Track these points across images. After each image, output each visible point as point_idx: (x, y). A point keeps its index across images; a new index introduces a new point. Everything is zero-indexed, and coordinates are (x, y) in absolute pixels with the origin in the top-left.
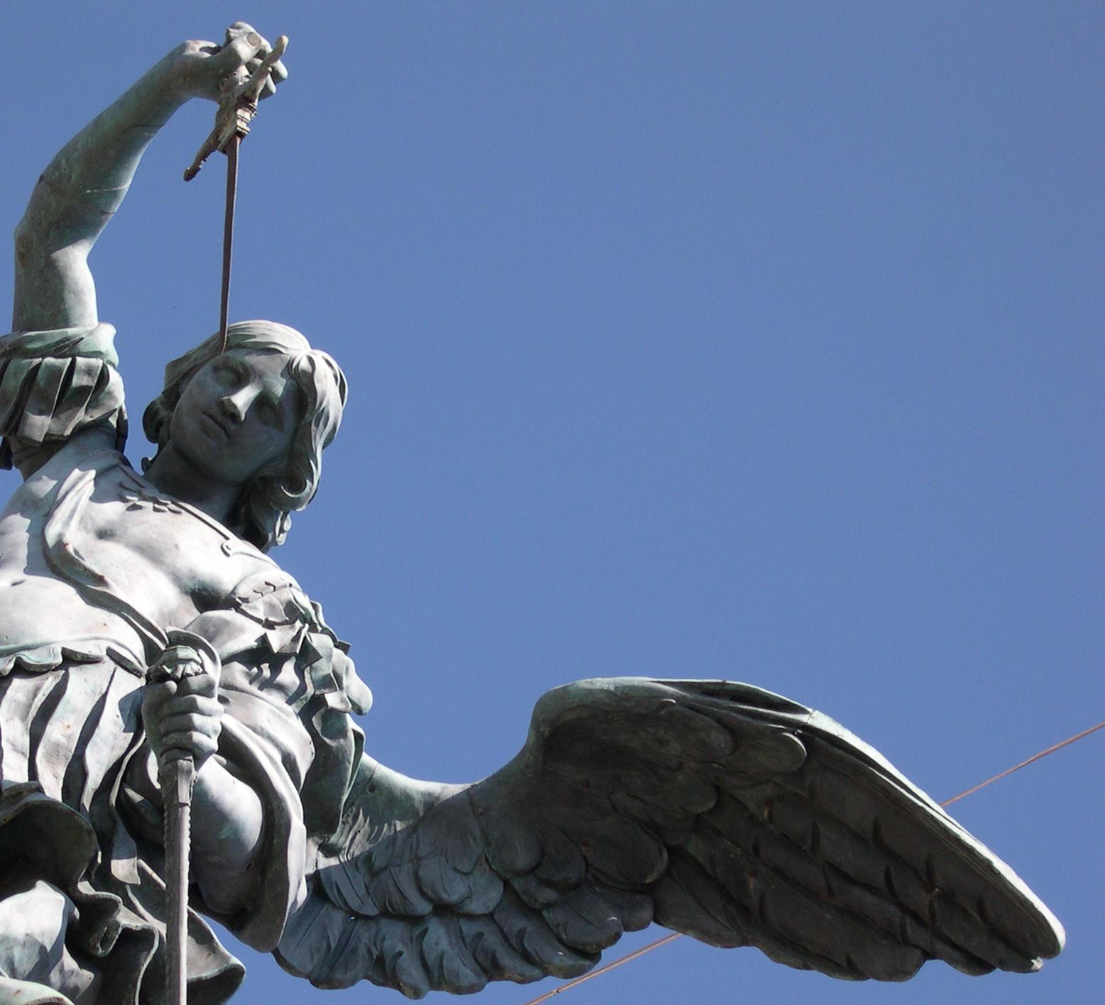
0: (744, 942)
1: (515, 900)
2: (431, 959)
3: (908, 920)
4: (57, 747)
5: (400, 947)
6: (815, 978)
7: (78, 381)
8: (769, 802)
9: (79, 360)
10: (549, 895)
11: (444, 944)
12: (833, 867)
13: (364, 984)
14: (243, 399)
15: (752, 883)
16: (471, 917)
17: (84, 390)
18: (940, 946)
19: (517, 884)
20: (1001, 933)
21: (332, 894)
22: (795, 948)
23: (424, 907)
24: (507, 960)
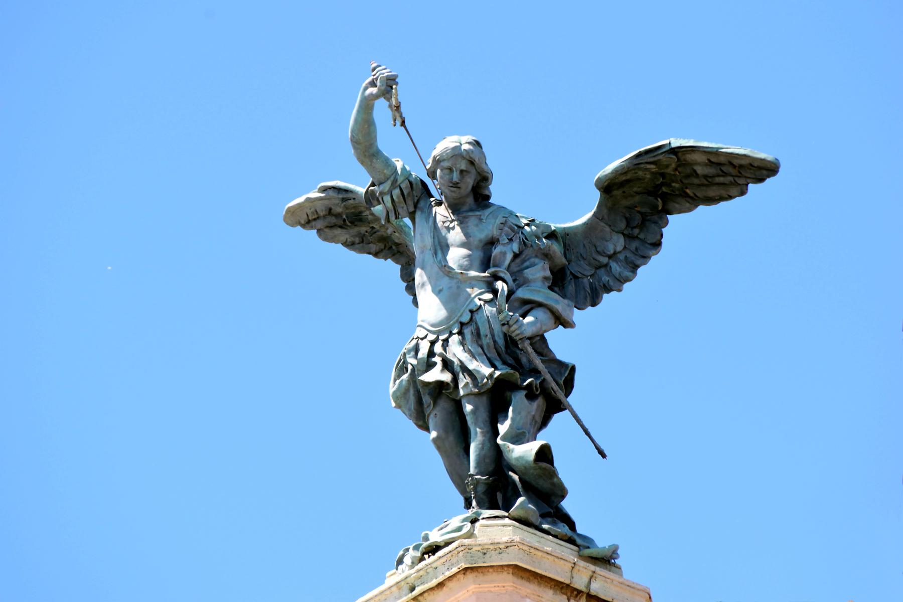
0: (697, 206)
1: (629, 237)
2: (617, 276)
3: (736, 179)
4: (488, 344)
5: (607, 279)
6: (723, 204)
7: (405, 194)
8: (676, 169)
9: (403, 186)
10: (636, 231)
11: (618, 269)
12: (706, 177)
13: (605, 296)
14: (456, 176)
15: (688, 191)
16: (620, 252)
17: (408, 194)
18: (749, 180)
19: (626, 232)
20: (764, 170)
21: (579, 275)
22: (710, 201)
23: (604, 260)
24: (638, 262)
